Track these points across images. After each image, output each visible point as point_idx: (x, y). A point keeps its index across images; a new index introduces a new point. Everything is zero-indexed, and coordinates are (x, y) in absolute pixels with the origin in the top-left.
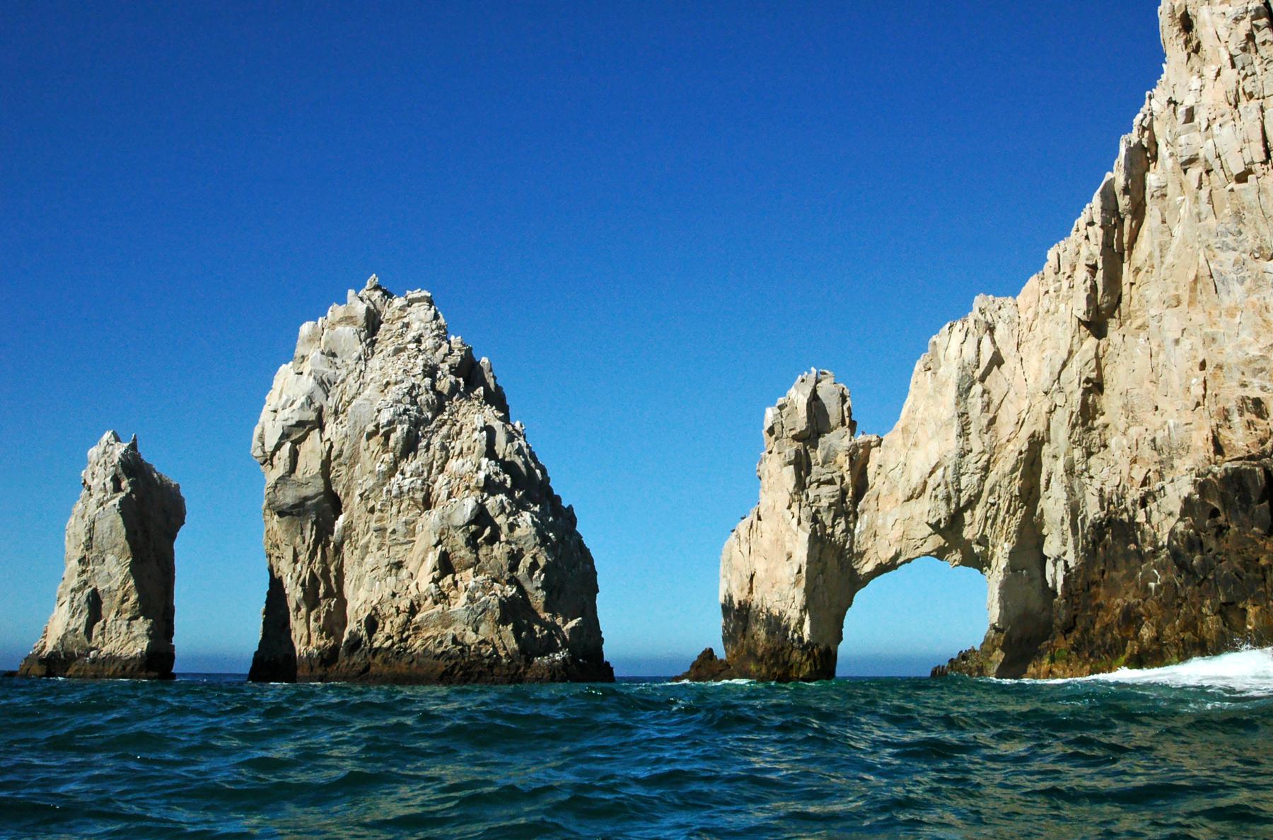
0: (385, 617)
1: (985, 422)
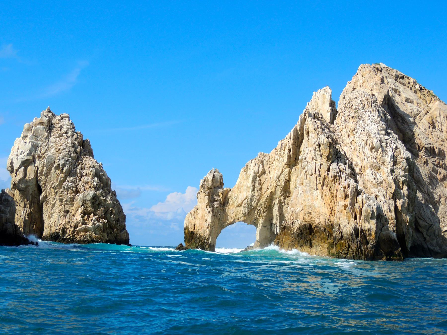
0: (67, 229)
1: (259, 188)
